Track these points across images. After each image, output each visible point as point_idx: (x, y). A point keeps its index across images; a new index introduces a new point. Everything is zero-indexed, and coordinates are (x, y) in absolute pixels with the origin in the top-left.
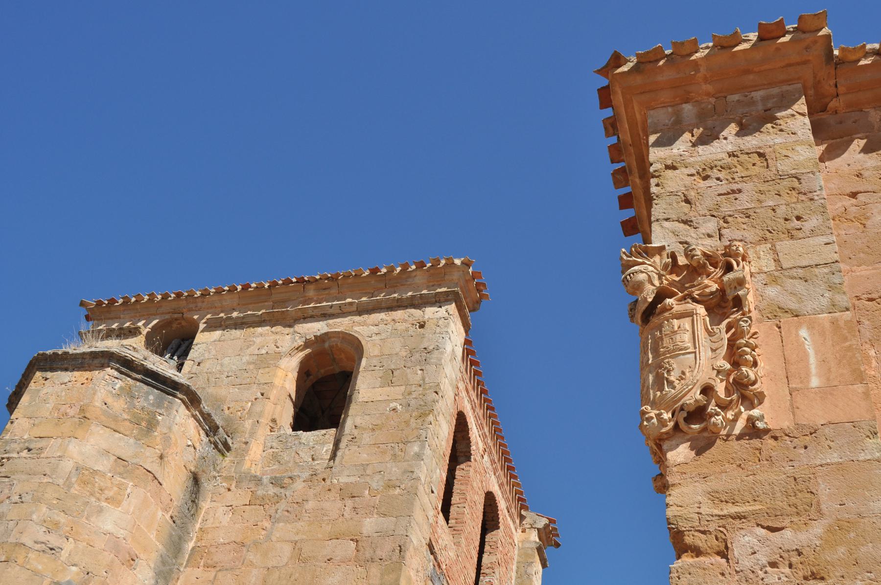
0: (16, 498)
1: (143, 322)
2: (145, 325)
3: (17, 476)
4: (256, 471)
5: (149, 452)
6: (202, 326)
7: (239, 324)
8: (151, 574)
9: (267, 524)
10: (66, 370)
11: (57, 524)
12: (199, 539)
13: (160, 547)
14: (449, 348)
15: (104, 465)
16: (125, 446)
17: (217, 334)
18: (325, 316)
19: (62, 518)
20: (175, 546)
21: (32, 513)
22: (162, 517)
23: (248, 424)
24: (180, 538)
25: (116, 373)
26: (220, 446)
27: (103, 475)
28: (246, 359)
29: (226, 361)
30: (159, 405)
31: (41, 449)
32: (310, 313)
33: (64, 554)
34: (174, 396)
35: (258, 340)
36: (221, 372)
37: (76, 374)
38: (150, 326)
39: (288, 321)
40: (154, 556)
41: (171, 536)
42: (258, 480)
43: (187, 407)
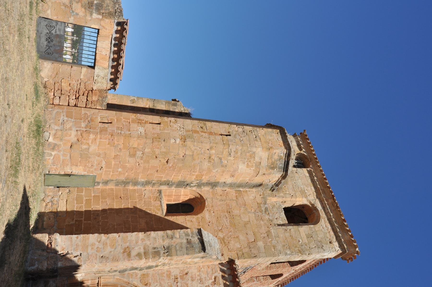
0: (241, 139)
1: (305, 150)
3: (248, 137)
4: (268, 202)
5: (265, 170)
6: (308, 169)
8: (230, 182)
9: (253, 211)
10: (282, 138)
11: (237, 153)
12: (244, 191)
13: (238, 182)
14: (325, 254)
15: (257, 159)
16: (265, 163)
17: (308, 175)
18: (324, 208)
19: (239, 154)
20: (240, 185)
21: (238, 145)
22: (247, 180)
23: (282, 194)
24: (242, 186)
25: (285, 153)
26: (273, 189)
27: (254, 160)
28: (302, 186)
29: (300, 181)
30: (279, 168)
31: (257, 140)
32: (323, 203)
33: (229, 158)
34: (283, 172)
35: (309, 188)
36: (296, 180)
37: (282, 142)
38: (304, 153)
39: (318, 196)
40: (235, 181)
41: (242, 184)
42: (265, 203)
43: (281, 176)
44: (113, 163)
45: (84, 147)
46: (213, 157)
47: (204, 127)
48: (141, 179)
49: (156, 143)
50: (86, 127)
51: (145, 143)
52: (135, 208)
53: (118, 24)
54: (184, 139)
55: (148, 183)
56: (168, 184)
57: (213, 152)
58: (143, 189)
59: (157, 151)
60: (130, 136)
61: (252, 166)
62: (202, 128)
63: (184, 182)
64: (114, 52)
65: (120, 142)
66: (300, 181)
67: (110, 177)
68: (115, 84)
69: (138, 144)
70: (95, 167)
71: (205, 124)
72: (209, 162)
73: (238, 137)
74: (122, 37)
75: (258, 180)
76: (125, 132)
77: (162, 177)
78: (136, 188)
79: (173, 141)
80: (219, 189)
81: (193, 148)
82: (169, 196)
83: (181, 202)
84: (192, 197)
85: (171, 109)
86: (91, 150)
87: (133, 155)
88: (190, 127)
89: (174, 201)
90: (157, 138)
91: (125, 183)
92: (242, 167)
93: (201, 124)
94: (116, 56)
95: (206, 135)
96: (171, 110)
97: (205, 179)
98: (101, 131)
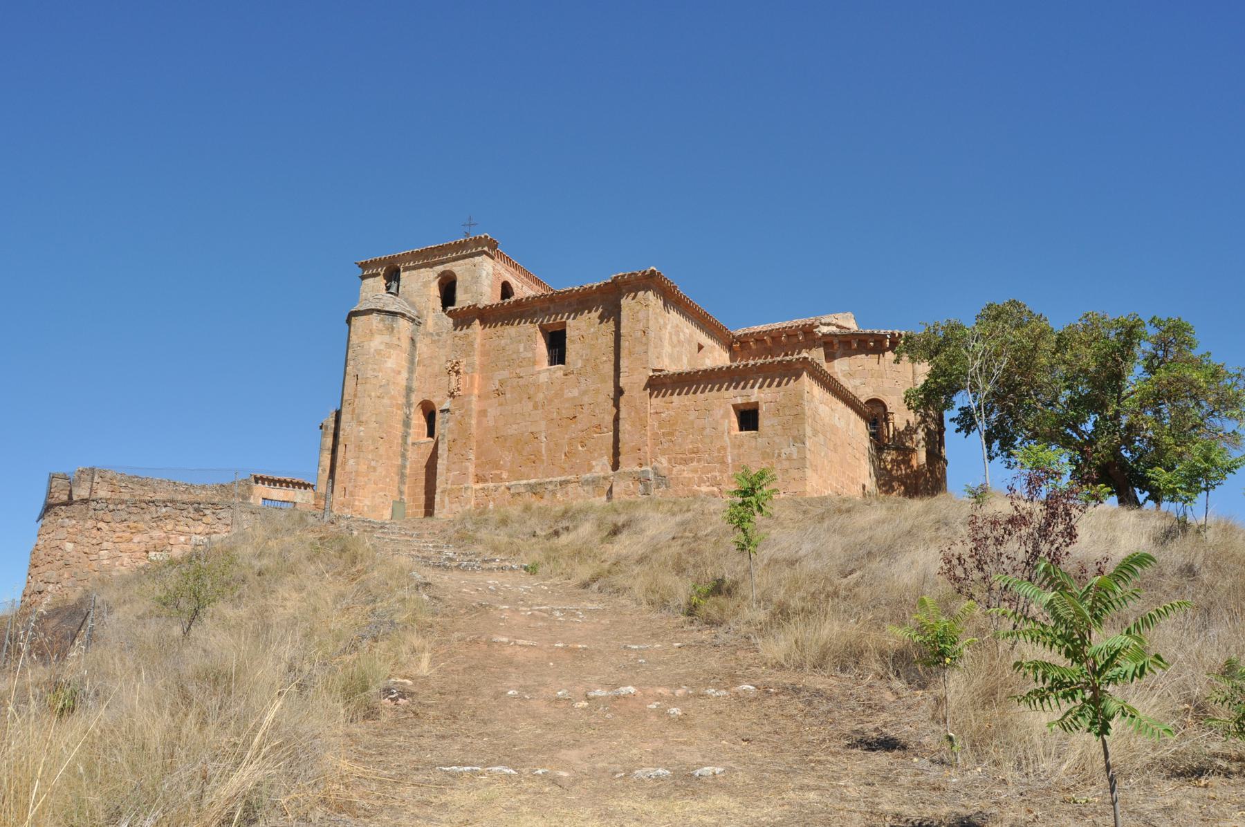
4: (431, 331)
5: (394, 338)
6: (402, 269)
7: (414, 268)
9: (437, 350)
14: (484, 274)
15: (382, 347)
16: (386, 338)
18: (442, 263)
19: (376, 367)
20: (412, 362)
22: (405, 356)
23: (425, 312)
28: (419, 284)
30: (393, 321)
35: (422, 275)
39: (431, 266)
42: (432, 334)
45: (366, 509)
46: (378, 394)
48: (399, 461)
49: (364, 449)
50: (348, 508)
52: (426, 466)
53: (257, 482)
54: (360, 423)
55: (403, 456)
57: (373, 394)
59: (371, 447)
63: (404, 421)
64: (281, 485)
65: (362, 480)
69: (364, 464)
72: (383, 398)
74: (267, 479)
75: (405, 344)
78: (408, 466)
79: (362, 434)
80: (415, 385)
81: (369, 414)
84: (421, 411)
87: (375, 469)
88: (349, 416)
89: (424, 430)
90: (359, 448)
91: (402, 476)
92: (390, 364)
93: (346, 404)
94: (284, 484)
95: (357, 400)
96: (332, 431)
97: (402, 400)
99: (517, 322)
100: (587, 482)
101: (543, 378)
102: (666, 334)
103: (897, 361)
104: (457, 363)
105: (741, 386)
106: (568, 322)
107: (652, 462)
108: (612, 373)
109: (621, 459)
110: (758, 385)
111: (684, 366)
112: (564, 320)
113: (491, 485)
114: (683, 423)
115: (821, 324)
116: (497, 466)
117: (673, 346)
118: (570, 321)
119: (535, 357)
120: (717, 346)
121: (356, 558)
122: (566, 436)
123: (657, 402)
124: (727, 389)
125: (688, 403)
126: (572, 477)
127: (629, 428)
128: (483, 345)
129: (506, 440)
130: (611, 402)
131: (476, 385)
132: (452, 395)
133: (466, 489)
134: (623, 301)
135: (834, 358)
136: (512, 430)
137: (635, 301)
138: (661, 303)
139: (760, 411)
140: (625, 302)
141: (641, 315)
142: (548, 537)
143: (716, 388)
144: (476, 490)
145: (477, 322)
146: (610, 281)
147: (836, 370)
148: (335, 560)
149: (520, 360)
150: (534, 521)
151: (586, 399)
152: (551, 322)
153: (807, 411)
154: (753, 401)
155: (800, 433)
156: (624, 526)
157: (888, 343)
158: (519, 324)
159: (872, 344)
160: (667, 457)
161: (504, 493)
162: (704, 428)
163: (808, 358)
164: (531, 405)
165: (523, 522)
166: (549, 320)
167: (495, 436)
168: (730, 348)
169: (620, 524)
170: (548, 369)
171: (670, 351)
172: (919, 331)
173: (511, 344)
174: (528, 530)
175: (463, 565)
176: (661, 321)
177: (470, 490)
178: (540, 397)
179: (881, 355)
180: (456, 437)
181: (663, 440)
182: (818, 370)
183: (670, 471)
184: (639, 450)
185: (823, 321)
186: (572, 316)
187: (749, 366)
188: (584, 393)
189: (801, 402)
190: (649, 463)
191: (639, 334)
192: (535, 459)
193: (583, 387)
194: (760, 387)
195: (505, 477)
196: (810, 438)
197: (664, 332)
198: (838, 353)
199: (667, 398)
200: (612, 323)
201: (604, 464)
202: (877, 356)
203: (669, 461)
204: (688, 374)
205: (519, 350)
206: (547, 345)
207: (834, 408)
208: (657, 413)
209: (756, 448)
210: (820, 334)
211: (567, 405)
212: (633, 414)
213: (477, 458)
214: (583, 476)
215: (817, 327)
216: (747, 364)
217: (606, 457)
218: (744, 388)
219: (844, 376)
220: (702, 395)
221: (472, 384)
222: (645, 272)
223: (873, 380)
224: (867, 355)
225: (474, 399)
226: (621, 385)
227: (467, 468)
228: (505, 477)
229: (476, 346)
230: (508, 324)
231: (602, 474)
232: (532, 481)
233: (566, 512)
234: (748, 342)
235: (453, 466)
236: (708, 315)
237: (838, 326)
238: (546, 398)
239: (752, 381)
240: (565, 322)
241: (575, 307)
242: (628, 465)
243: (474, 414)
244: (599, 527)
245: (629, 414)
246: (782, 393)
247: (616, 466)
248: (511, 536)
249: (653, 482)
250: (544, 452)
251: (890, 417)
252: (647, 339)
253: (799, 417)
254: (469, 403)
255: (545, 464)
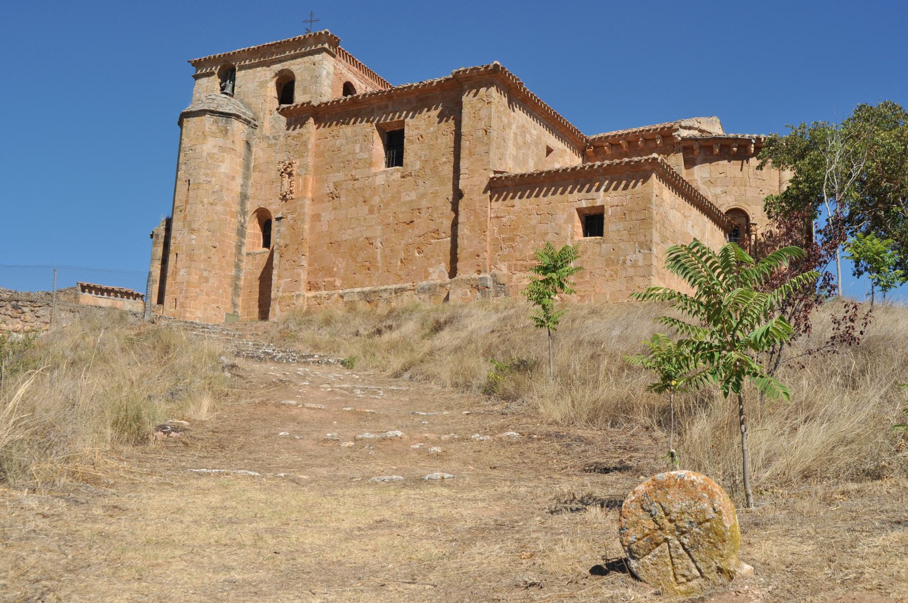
2: (216, 69)
5: (228, 141)
6: (237, 68)
7: (250, 67)
9: (274, 154)
14: (324, 73)
15: (215, 151)
16: (220, 141)
17: (243, 71)
18: (280, 61)
19: (209, 172)
20: (247, 167)
23: (262, 114)
28: (256, 84)
29: (249, 85)
35: (258, 74)
36: (248, 91)
40: (241, 174)
42: (268, 138)
44: (213, 297)
46: (211, 201)
47: (181, 208)
48: (233, 272)
51: (195, 268)
53: (83, 291)
54: (192, 231)
55: (238, 266)
56: (239, 247)
57: (205, 200)
58: (244, 271)
59: (204, 257)
60: (188, 282)
61: (223, 156)
62: (181, 211)
63: (238, 230)
64: (109, 295)
65: (193, 291)
66: (249, 85)
67: (229, 301)
68: (138, 296)
70: (217, 313)
71: (177, 207)
72: (216, 204)
73: (191, 171)
74: (94, 288)
75: (240, 148)
76: (184, 287)
77: (231, 253)
78: (242, 278)
79: (193, 242)
80: (250, 192)
81: (202, 221)
82: (254, 245)
83: (261, 233)
84: (256, 220)
85: (161, 240)
86: (200, 316)
87: (207, 280)
88: (181, 224)
89: (260, 240)
90: (191, 257)
91: (236, 287)
92: (224, 168)
93: (177, 211)
94: (112, 294)
97: (236, 208)
98: (183, 307)
99: (353, 120)
100: (423, 290)
101: (380, 180)
102: (510, 134)
103: (760, 167)
104: (290, 164)
105: (585, 189)
106: (406, 120)
107: (491, 269)
108: (451, 175)
109: (459, 265)
110: (603, 188)
111: (530, 167)
112: (402, 119)
113: (324, 293)
114: (524, 227)
115: (681, 127)
116: (330, 272)
117: (519, 148)
118: (408, 120)
119: (371, 158)
120: (568, 150)
121: (168, 347)
122: (403, 242)
123: (498, 205)
124: (571, 192)
125: (530, 207)
126: (408, 285)
127: (468, 233)
128: (317, 146)
129: (340, 246)
130: (450, 206)
131: (310, 189)
132: (284, 198)
133: (298, 296)
134: (464, 98)
135: (694, 165)
136: (347, 235)
137: (476, 98)
138: (505, 100)
139: (605, 215)
140: (467, 99)
141: (483, 113)
142: (370, 336)
143: (560, 191)
144: (308, 298)
145: (311, 120)
146: (451, 76)
147: (696, 177)
148: (148, 351)
149: (356, 161)
150: (358, 320)
151: (424, 203)
152: (388, 121)
153: (655, 215)
154: (598, 204)
155: (647, 238)
156: (446, 323)
157: (753, 149)
158: (354, 123)
159: (735, 149)
160: (506, 263)
161: (337, 301)
162: (546, 234)
163: (657, 159)
164: (366, 209)
165: (346, 322)
166: (386, 118)
167: (329, 241)
168: (583, 153)
169: (442, 320)
170: (385, 171)
171: (514, 152)
172: (784, 135)
173: (347, 144)
174: (354, 330)
175: (278, 357)
176: (505, 120)
177: (301, 298)
178: (376, 200)
179: (745, 162)
180: (288, 243)
181: (504, 246)
182: (669, 174)
183: (510, 279)
184: (478, 256)
185: (683, 124)
186: (411, 115)
187: (596, 167)
188: (423, 196)
189: (648, 205)
190: (488, 269)
191: (481, 132)
192: (369, 266)
193: (421, 190)
194: (606, 191)
195: (339, 285)
196: (658, 244)
197: (508, 131)
198: (699, 159)
199: (508, 202)
200: (451, 122)
201: (441, 271)
202: (740, 162)
203: (509, 268)
204: (531, 175)
205: (354, 150)
206: (384, 145)
207: (687, 214)
208: (497, 217)
209: (600, 255)
210: (680, 138)
211: (403, 209)
212: (472, 218)
213: (310, 265)
214: (420, 284)
215: (677, 130)
216: (594, 165)
217: (443, 264)
218: (588, 191)
219: (704, 183)
220: (546, 198)
221: (305, 186)
222: (488, 66)
223: (736, 188)
224: (729, 161)
225: (308, 202)
226: (460, 187)
227: (299, 275)
228: (339, 285)
229: (310, 147)
230: (343, 123)
231: (439, 282)
232: (367, 289)
233: (391, 312)
234: (603, 146)
235: (285, 273)
236: (558, 116)
237: (701, 131)
238: (382, 201)
239: (597, 184)
240: (403, 121)
241: (415, 104)
242: (466, 272)
243: (307, 219)
244: (423, 325)
245: (468, 218)
246: (629, 197)
247: (453, 273)
248: (332, 335)
249: (492, 289)
250: (379, 259)
251: (753, 228)
252: (489, 138)
253: (646, 221)
254: (302, 206)
255: (380, 271)
